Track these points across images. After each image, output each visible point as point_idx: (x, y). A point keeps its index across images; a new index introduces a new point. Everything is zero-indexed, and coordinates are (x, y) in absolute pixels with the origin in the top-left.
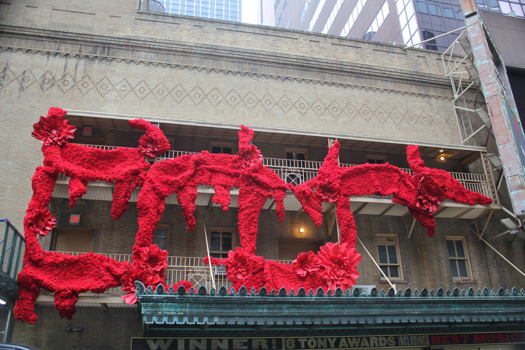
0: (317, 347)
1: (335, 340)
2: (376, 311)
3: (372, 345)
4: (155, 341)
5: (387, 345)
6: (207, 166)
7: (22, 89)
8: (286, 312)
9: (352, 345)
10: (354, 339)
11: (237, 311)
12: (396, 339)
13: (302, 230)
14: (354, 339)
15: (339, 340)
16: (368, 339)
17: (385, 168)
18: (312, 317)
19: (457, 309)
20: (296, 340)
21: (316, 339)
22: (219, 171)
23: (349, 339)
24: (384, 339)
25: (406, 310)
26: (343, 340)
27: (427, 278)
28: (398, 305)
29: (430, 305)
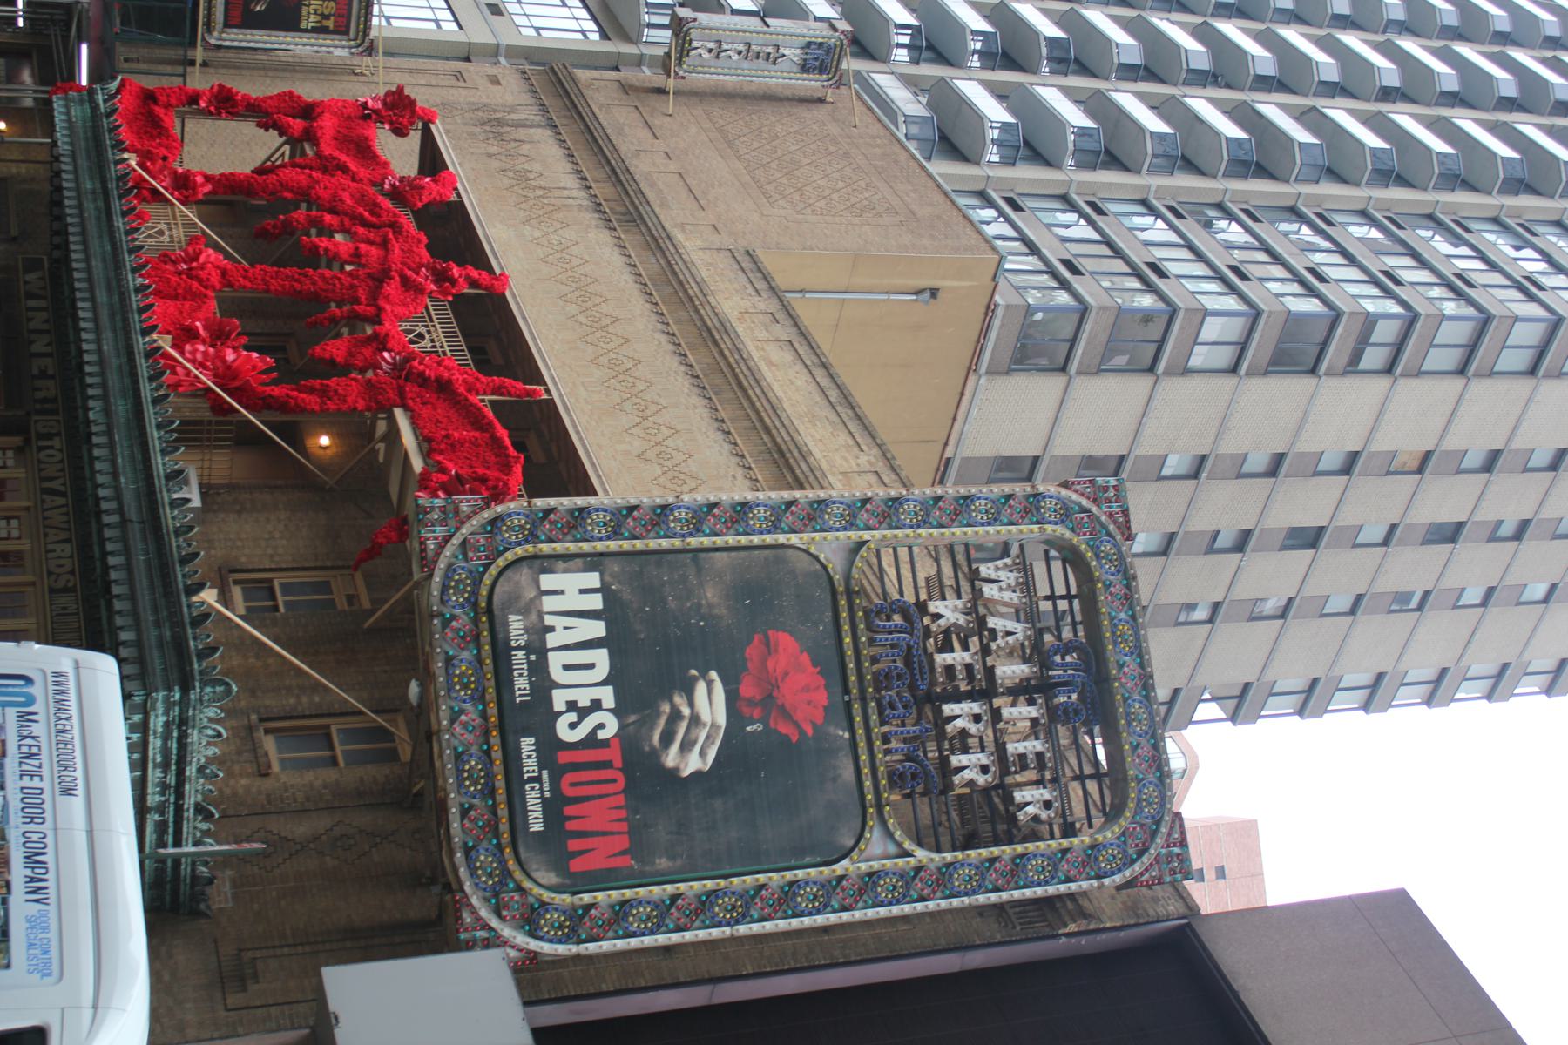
0: (40, 462)
1: (62, 489)
2: (102, 297)
3: (50, 547)
4: (42, 278)
5: (50, 573)
6: (391, 235)
7: (490, 155)
8: (89, 206)
9: (47, 514)
10: (65, 518)
11: (83, 163)
12: (65, 590)
13: (325, 441)
14: (65, 518)
15: (63, 494)
16: (68, 541)
17: (508, 456)
18: (83, 233)
19: (121, 408)
20: (58, 434)
21: (61, 461)
22: (387, 250)
23: (64, 510)
24: (68, 568)
25: (107, 335)
26: (62, 501)
27: (252, 660)
28: (119, 325)
29: (126, 369)
